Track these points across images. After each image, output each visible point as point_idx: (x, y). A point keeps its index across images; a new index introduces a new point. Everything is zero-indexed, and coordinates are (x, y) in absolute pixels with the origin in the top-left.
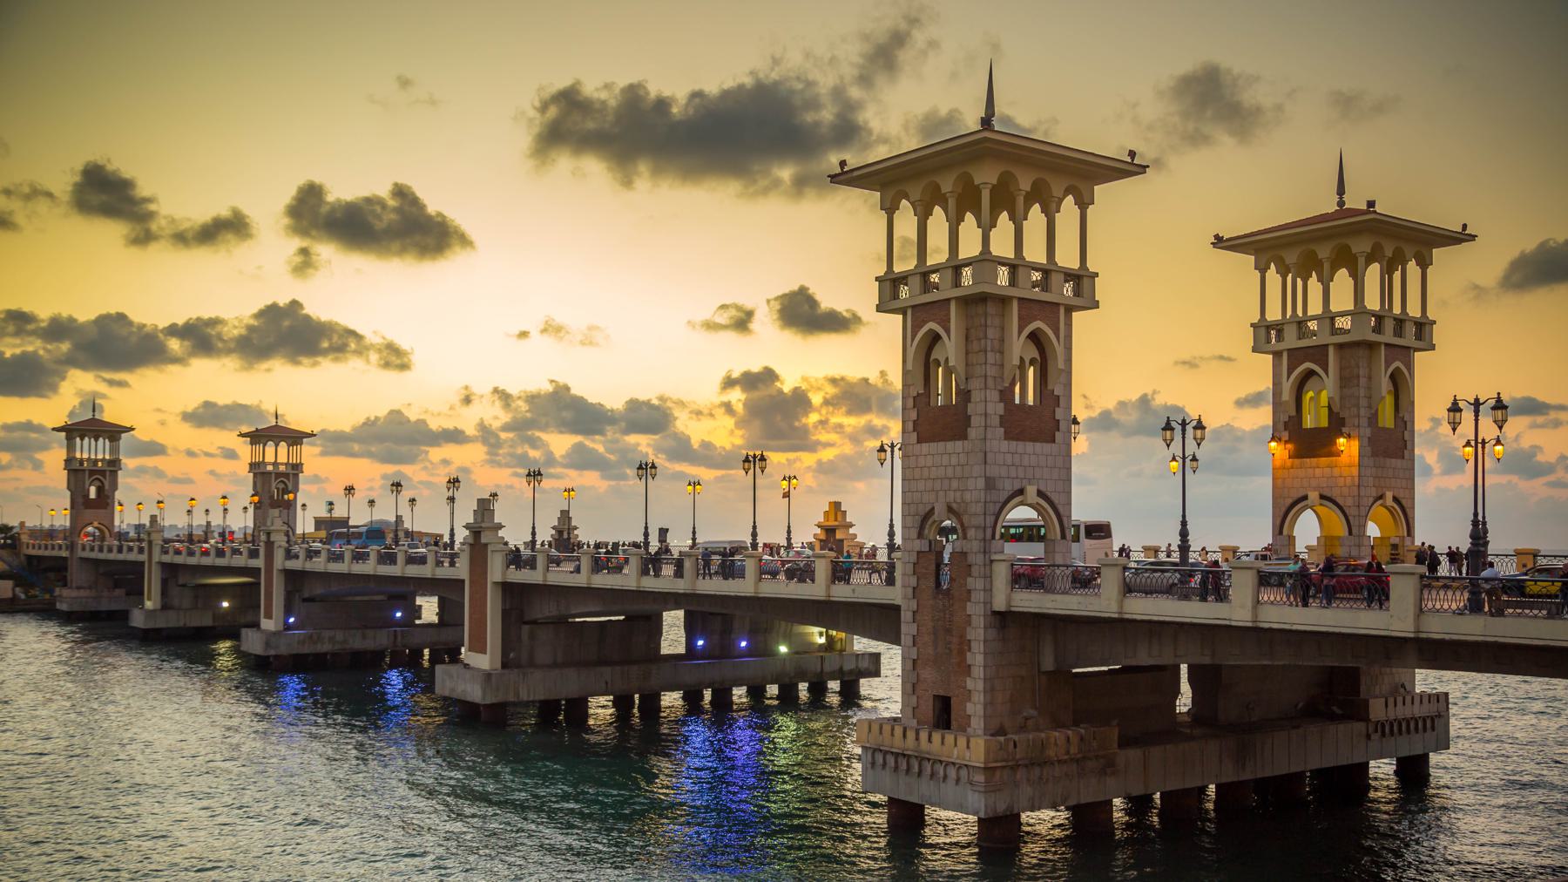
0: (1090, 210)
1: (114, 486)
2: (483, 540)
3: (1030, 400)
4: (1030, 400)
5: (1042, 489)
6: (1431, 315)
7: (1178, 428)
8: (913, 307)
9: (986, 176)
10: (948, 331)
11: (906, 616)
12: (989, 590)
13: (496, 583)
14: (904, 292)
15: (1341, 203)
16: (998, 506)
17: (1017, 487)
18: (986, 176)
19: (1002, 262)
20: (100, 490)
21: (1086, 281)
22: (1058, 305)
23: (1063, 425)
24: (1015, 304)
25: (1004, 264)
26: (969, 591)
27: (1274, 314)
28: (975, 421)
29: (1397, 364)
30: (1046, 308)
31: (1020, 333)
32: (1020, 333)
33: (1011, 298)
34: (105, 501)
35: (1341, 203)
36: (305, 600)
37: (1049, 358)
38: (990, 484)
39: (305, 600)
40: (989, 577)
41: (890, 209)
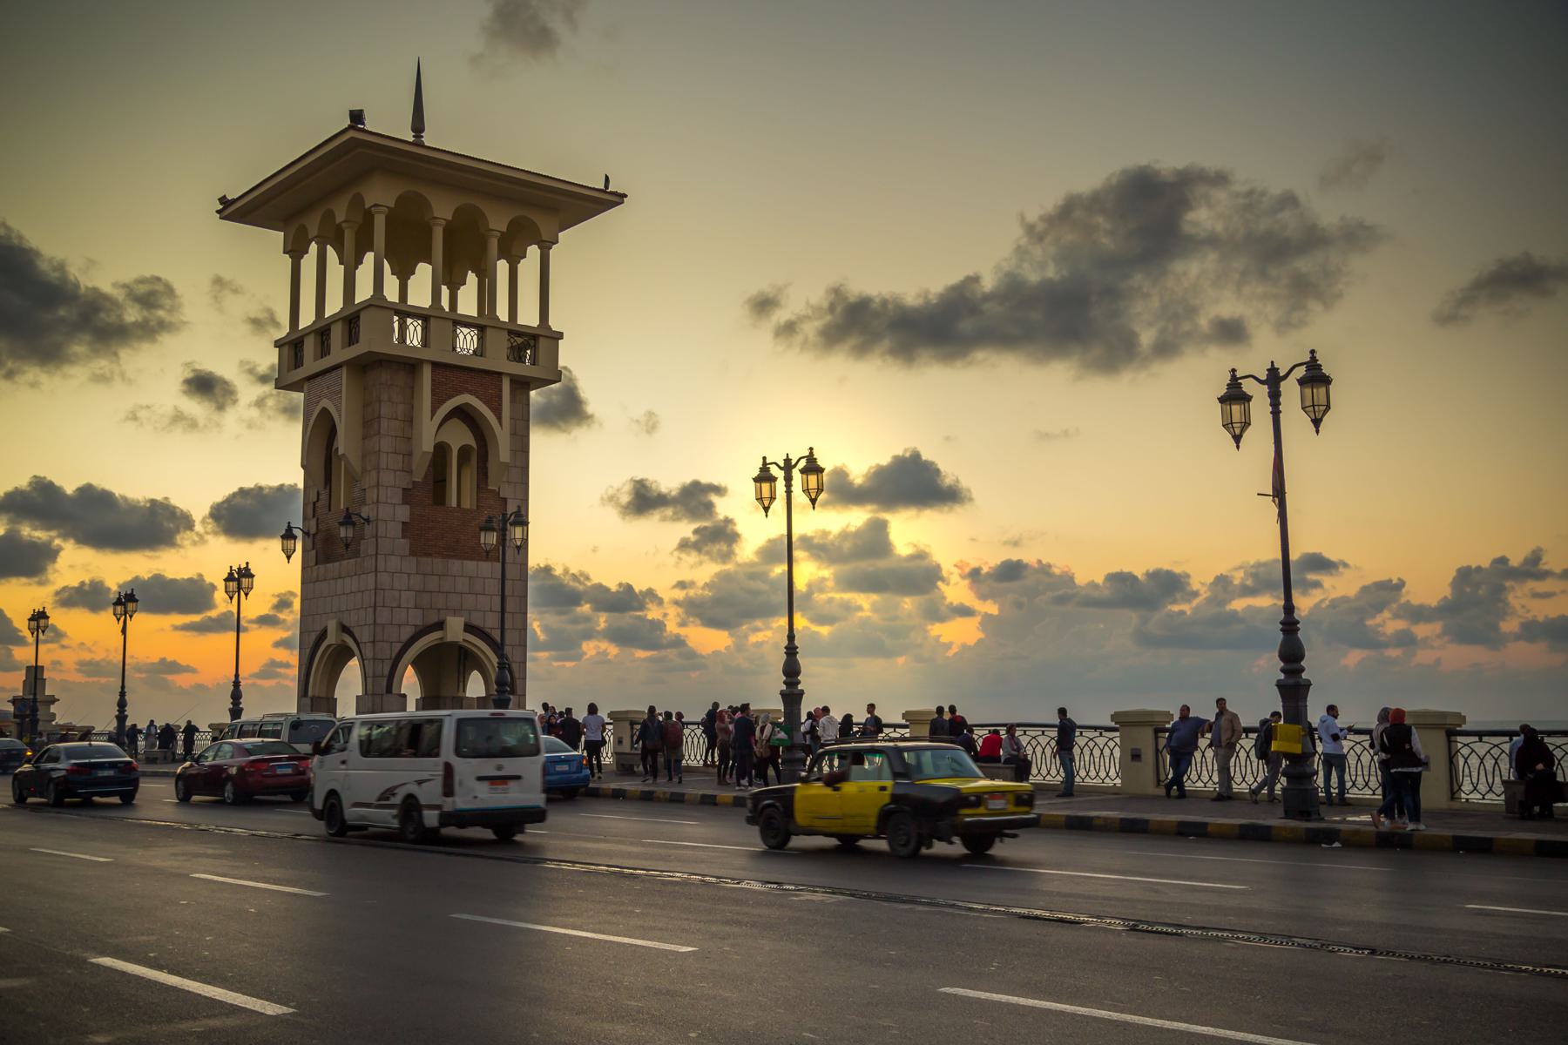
0: (554, 252)
3: (467, 504)
4: (466, 504)
5: (477, 622)
9: (381, 195)
16: (397, 647)
17: (433, 618)
18: (381, 195)
19: (467, 322)
21: (542, 343)
22: (500, 374)
24: (427, 373)
25: (467, 325)
30: (518, 378)
31: (433, 412)
32: (433, 412)
33: (421, 362)
41: (295, 251)
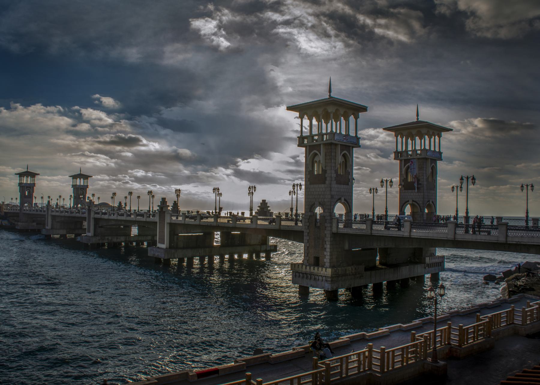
1: (33, 192)
2: (164, 210)
6: (441, 151)
7: (385, 182)
8: (309, 146)
10: (320, 153)
11: (305, 234)
12: (331, 227)
13: (168, 223)
14: (306, 141)
15: (418, 119)
20: (29, 192)
23: (351, 180)
26: (326, 227)
27: (400, 149)
28: (328, 179)
29: (433, 164)
34: (31, 196)
35: (418, 119)
36: (100, 227)
37: (347, 163)
38: (332, 197)
39: (100, 227)
40: (331, 223)
